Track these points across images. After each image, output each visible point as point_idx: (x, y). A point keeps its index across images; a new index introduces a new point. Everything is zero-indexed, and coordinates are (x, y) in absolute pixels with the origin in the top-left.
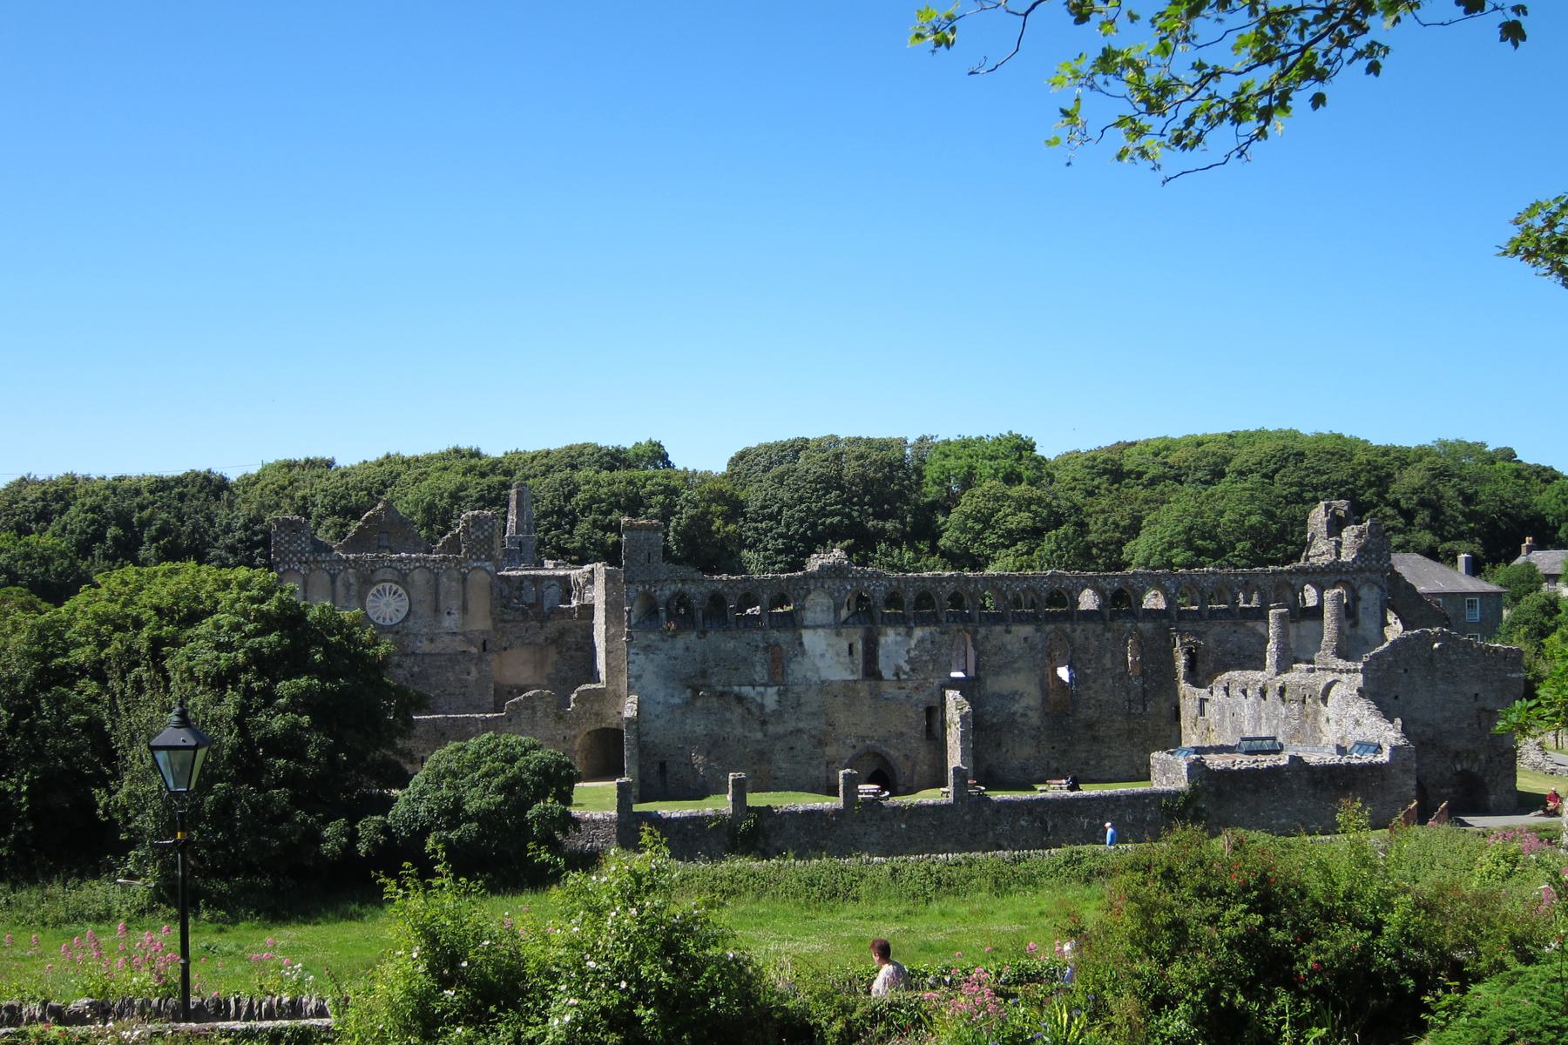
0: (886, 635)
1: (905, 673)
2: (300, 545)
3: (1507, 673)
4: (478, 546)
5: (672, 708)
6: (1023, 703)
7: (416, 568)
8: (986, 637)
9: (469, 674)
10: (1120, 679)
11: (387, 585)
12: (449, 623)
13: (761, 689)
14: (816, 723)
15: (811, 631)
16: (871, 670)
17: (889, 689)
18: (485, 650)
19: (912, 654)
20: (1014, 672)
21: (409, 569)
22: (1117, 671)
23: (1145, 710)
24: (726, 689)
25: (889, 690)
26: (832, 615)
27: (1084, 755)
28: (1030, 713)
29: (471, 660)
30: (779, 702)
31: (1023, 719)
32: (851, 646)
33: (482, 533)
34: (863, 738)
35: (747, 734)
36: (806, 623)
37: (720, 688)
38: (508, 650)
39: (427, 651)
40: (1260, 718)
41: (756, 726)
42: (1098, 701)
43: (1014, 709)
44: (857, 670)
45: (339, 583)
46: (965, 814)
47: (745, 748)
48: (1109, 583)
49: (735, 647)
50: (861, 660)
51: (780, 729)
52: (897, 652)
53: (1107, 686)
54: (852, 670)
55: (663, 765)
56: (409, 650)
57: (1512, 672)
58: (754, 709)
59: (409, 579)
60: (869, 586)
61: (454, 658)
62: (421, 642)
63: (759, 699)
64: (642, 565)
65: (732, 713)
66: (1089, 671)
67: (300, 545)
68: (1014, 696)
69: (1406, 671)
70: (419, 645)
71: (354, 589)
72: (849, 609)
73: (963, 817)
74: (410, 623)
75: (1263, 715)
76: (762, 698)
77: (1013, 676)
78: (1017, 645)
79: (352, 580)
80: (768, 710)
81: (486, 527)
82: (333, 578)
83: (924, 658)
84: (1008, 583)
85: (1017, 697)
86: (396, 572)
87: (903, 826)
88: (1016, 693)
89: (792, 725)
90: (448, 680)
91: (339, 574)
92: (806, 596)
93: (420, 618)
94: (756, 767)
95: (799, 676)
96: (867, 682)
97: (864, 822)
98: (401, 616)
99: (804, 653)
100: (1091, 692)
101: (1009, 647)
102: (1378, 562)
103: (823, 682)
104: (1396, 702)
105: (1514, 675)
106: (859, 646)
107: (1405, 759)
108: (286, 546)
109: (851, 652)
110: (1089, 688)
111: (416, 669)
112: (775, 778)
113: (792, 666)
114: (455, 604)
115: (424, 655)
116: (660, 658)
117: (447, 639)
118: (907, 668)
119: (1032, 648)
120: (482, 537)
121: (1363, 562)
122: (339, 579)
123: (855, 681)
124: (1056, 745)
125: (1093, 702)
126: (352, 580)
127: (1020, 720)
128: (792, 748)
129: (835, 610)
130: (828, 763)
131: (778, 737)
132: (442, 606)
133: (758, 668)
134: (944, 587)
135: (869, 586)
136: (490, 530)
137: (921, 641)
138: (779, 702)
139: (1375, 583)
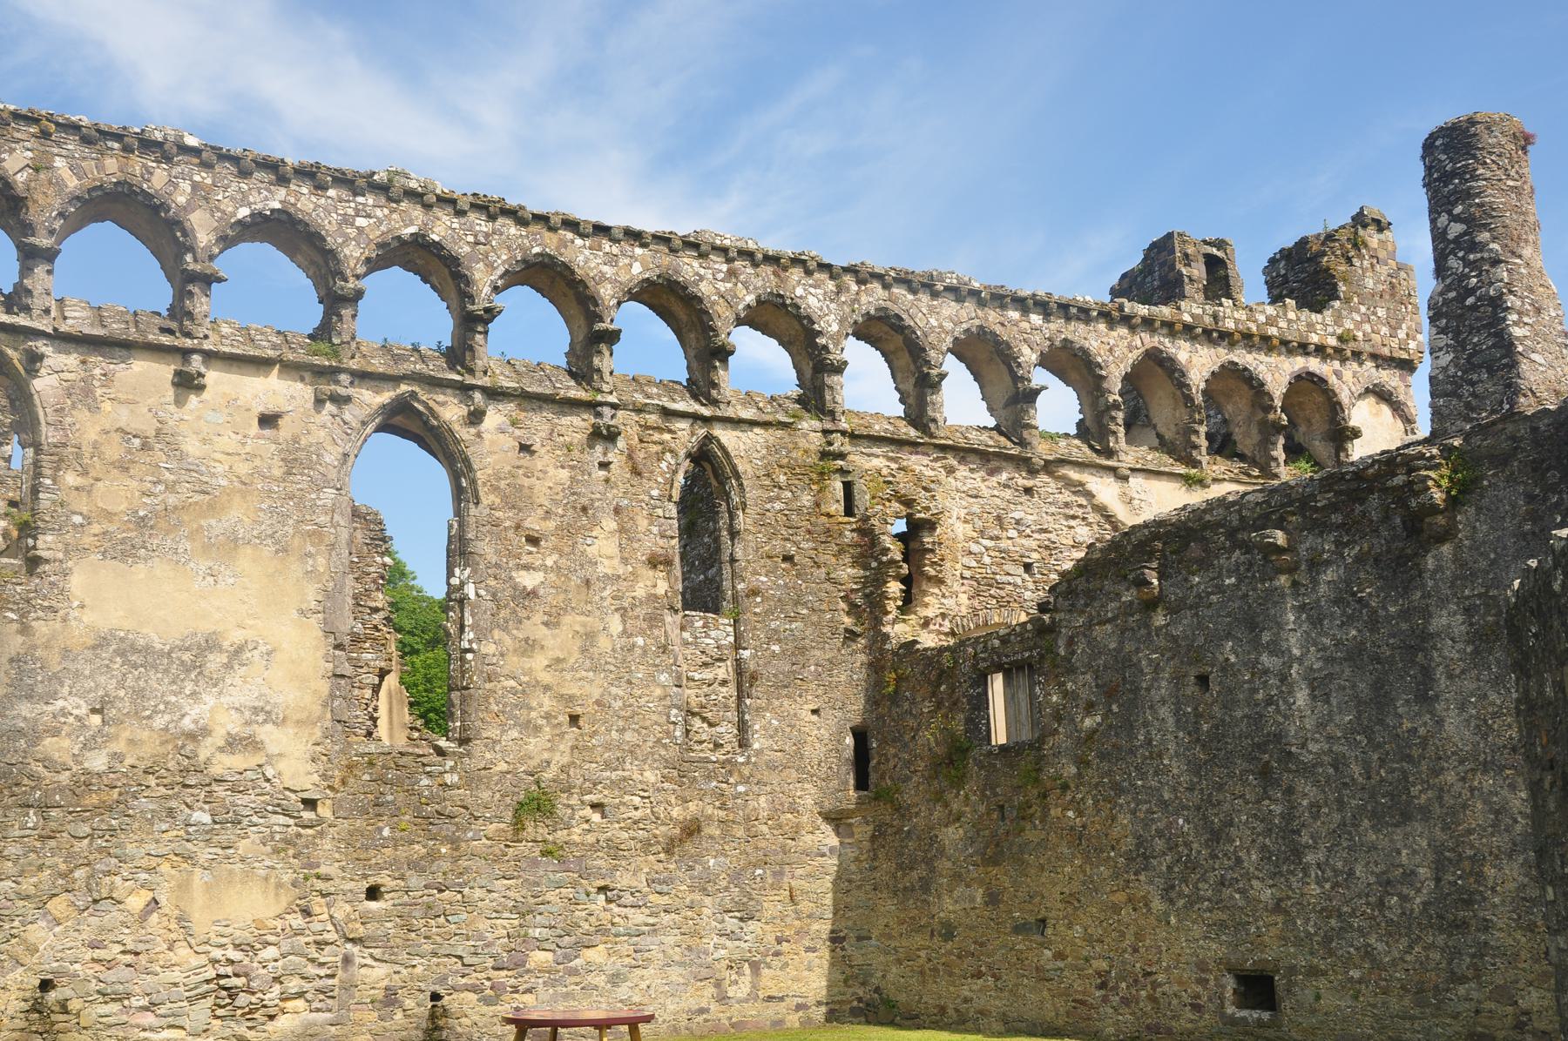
6: (242, 690)
20: (207, 549)
22: (640, 592)
23: (743, 744)
27: (509, 922)
28: (266, 733)
31: (237, 761)
40: (1419, 642)
48: (612, 260)
53: (604, 643)
66: (528, 580)
75: (1449, 620)
78: (228, 441)
84: (202, 177)
85: (215, 661)
88: (211, 644)
100: (539, 661)
101: (192, 447)
119: (295, 460)
124: (385, 880)
125: (547, 703)
127: (225, 764)
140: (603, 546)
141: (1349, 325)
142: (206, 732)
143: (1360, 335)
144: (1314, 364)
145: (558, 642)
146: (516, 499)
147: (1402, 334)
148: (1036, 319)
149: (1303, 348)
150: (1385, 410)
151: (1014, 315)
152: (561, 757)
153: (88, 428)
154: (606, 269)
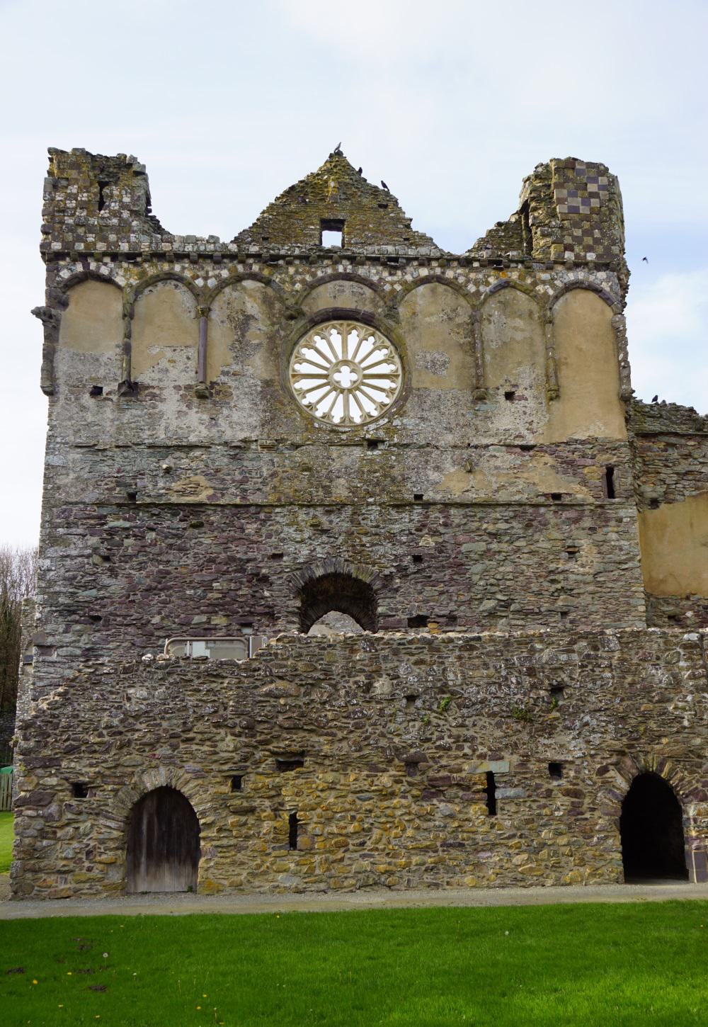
4: (578, 232)
9: (572, 553)
18: (611, 494)
21: (403, 283)
29: (577, 521)
33: (586, 202)
38: (663, 506)
39: (456, 496)
45: (216, 315)
59: (402, 311)
62: (437, 468)
67: (115, 214)
71: (259, 330)
74: (409, 422)
79: (253, 307)
82: (204, 301)
86: (368, 292)
90: (518, 574)
93: (435, 406)
111: (428, 542)
114: (527, 377)
115: (447, 505)
117: (507, 460)
120: (584, 210)
122: (216, 306)
126: (253, 307)
132: (494, 379)
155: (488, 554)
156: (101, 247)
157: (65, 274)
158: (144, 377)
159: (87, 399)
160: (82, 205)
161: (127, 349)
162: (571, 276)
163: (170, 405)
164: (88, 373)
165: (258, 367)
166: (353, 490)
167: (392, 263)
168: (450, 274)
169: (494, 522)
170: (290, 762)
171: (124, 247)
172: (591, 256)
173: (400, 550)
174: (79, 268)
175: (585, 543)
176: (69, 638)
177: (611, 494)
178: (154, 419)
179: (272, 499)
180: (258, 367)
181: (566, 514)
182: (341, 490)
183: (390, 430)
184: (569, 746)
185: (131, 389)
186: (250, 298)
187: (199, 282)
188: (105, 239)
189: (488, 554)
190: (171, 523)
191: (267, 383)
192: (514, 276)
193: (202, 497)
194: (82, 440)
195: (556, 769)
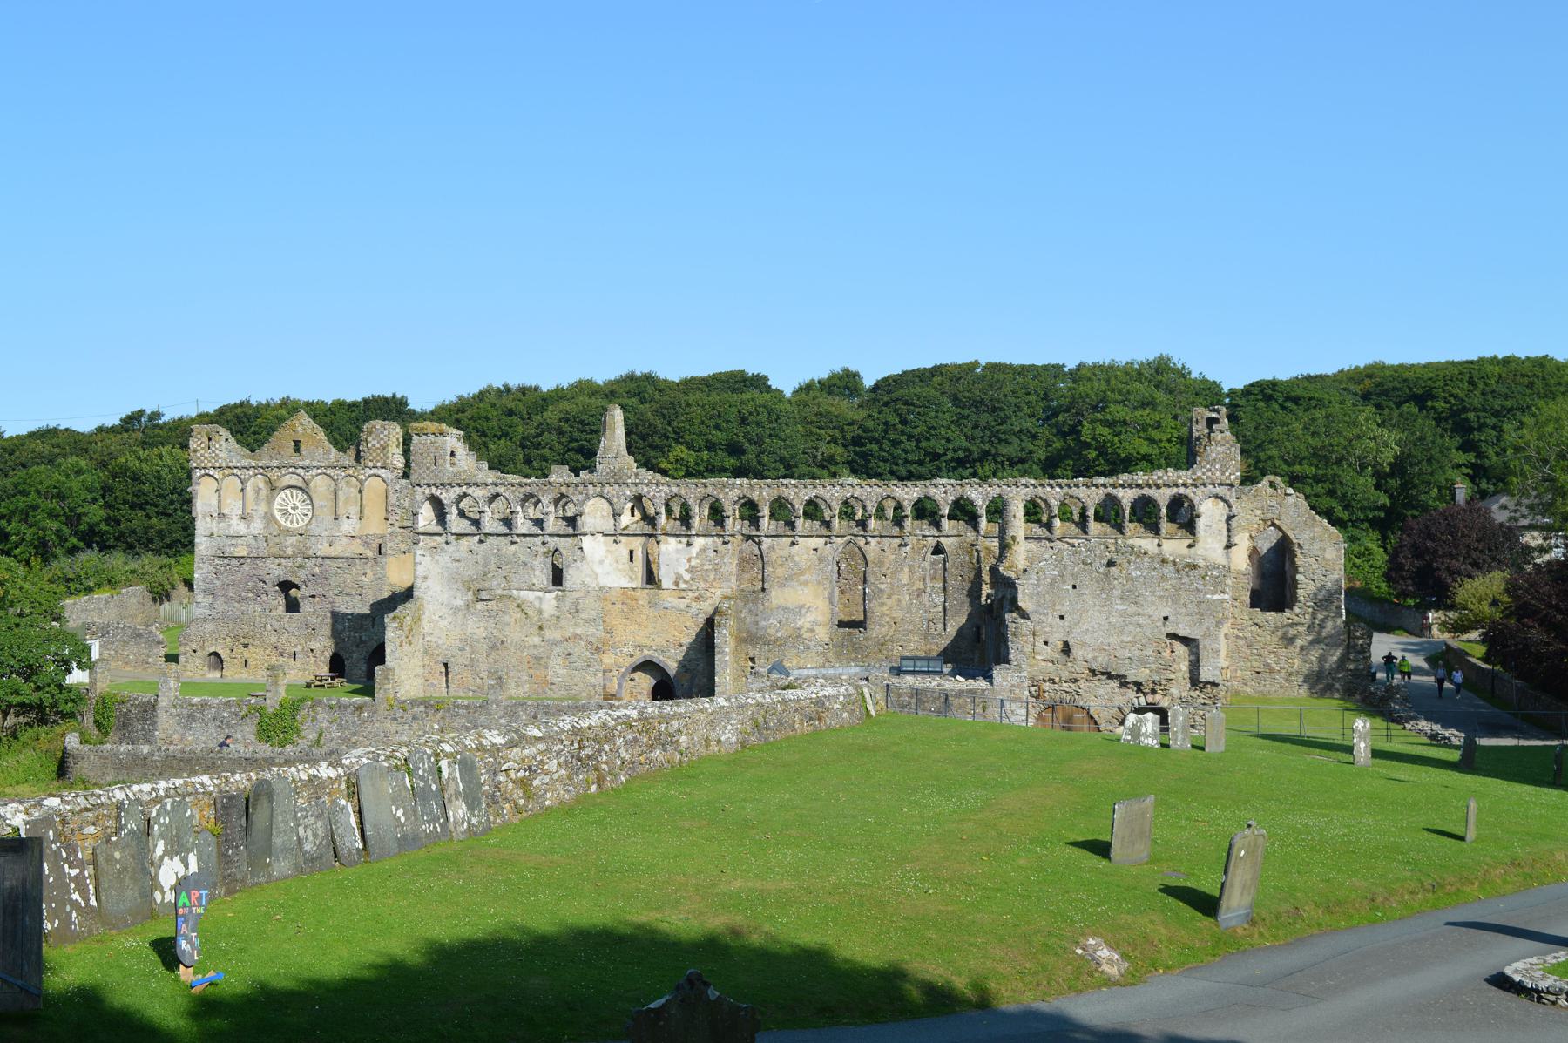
0: (667, 543)
1: (686, 582)
2: (213, 452)
3: (1206, 594)
4: (374, 455)
5: (455, 610)
6: (810, 617)
7: (317, 475)
8: (772, 548)
9: (365, 574)
10: (918, 596)
11: (294, 491)
12: (348, 526)
13: (540, 594)
14: (592, 630)
15: (589, 537)
16: (651, 578)
17: (668, 598)
18: (380, 554)
19: (693, 563)
22: (915, 588)
24: (505, 592)
25: (669, 599)
26: (612, 521)
28: (816, 628)
30: (557, 607)
32: (631, 552)
34: (641, 647)
35: (523, 638)
36: (586, 529)
37: (499, 592)
41: (535, 630)
42: (894, 618)
43: (799, 624)
44: (636, 578)
45: (249, 488)
46: (501, 718)
47: (522, 652)
48: (907, 493)
49: (516, 552)
50: (640, 569)
51: (557, 635)
52: (677, 560)
53: (904, 603)
54: (631, 578)
55: (446, 665)
56: (311, 553)
57: (1215, 593)
58: (530, 612)
60: (649, 492)
61: (350, 560)
63: (537, 604)
64: (428, 468)
65: (511, 617)
66: (883, 587)
67: (213, 452)
68: (800, 610)
69: (1074, 587)
70: (320, 547)
72: (633, 515)
73: (497, 721)
76: (541, 603)
77: (799, 588)
78: (805, 557)
79: (261, 485)
80: (546, 615)
81: (382, 436)
83: (705, 567)
85: (803, 611)
87: (436, 726)
88: (802, 606)
89: (569, 632)
91: (249, 479)
92: (584, 501)
94: (532, 671)
95: (579, 582)
96: (646, 591)
97: (396, 719)
98: (307, 519)
99: (583, 558)
100: (885, 608)
101: (796, 559)
102: (1223, 473)
103: (601, 588)
104: (1061, 622)
105: (1216, 597)
106: (639, 555)
107: (1013, 686)
108: (202, 452)
109: (631, 560)
110: (883, 604)
111: (317, 570)
112: (552, 684)
113: (571, 571)
116: (444, 559)
117: (345, 541)
118: (687, 577)
119: (821, 561)
120: (378, 446)
121: (1204, 474)
123: (634, 589)
127: (806, 635)
128: (569, 654)
129: (614, 516)
130: (605, 672)
131: (556, 643)
132: (341, 511)
133: (538, 573)
134: (727, 494)
135: (649, 492)
136: (386, 439)
137: (703, 550)
138: (557, 607)
139: (1221, 498)
140: (904, 576)
141: (1199, 474)
142: (802, 627)
143: (1204, 477)
144: (1182, 490)
145: (889, 603)
146: (880, 564)
147: (1227, 474)
148: (1058, 489)
149: (1176, 485)
150: (1222, 503)
151: (1049, 489)
152: (890, 634)
153: (774, 557)
154: (906, 497)
155: (336, 574)
156: (210, 465)
157: (198, 474)
158: (226, 511)
159: (208, 519)
160: (203, 449)
161: (219, 501)
162: (372, 472)
163: (235, 521)
164: (207, 510)
165: (263, 508)
166: (293, 552)
167: (307, 468)
168: (328, 472)
169: (340, 563)
170: (246, 646)
171: (217, 465)
172: (379, 464)
173: (307, 573)
174: (203, 472)
175: (368, 571)
176: (205, 600)
177: (380, 554)
178: (230, 526)
179: (266, 554)
180: (263, 508)
181: (363, 561)
182: (289, 552)
183: (306, 531)
184: (315, 645)
185: (221, 516)
186: (260, 481)
187: (242, 477)
188: (210, 461)
189: (336, 574)
190: (234, 562)
191: (266, 513)
192: (351, 471)
193: (245, 554)
194: (208, 533)
195: (312, 650)
